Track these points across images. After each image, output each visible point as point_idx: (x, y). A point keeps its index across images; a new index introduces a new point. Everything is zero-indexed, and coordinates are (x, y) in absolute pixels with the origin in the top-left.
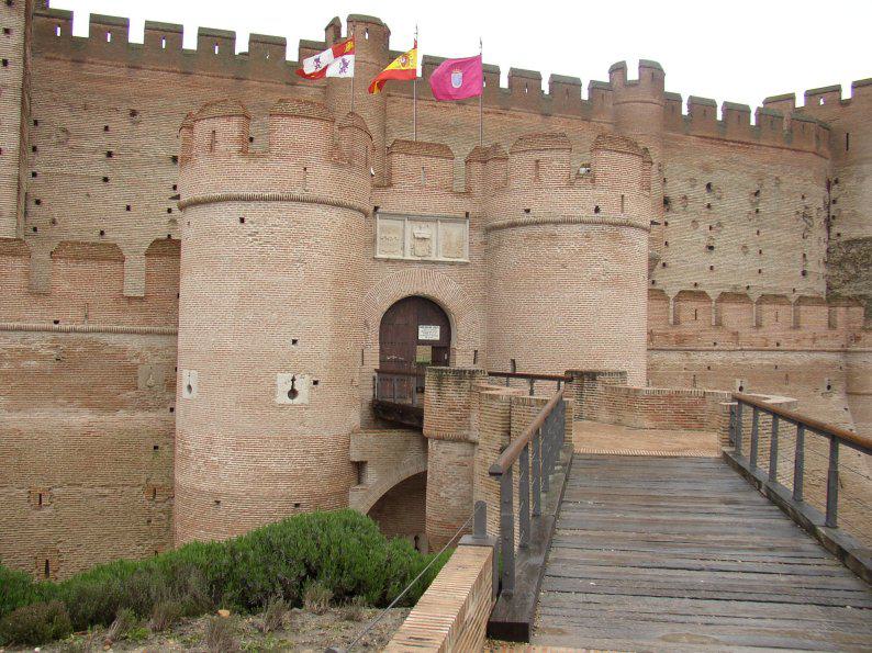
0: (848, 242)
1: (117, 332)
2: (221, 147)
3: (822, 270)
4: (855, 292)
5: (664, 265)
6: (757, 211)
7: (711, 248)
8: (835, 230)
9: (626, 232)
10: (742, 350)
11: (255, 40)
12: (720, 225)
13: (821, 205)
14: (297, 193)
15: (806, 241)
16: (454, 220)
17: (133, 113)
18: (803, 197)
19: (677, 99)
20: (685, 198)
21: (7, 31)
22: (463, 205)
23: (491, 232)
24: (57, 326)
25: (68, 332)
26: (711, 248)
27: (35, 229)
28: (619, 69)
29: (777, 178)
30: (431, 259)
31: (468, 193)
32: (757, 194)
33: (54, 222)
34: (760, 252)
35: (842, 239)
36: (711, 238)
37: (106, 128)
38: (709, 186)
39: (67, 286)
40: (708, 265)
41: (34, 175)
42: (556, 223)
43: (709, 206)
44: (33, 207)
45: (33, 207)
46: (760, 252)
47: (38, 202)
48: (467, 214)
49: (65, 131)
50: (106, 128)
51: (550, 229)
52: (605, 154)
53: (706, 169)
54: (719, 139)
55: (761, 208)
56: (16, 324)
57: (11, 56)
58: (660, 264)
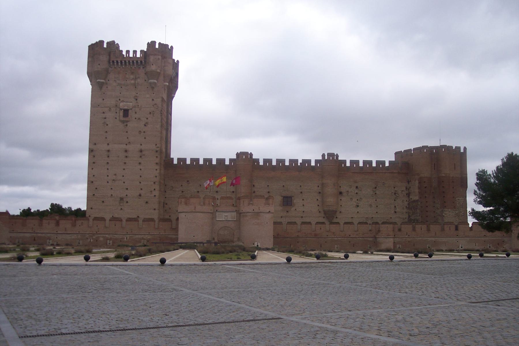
0: (413, 201)
1: (170, 235)
2: (182, 203)
3: (405, 210)
4: (414, 218)
5: (340, 212)
6: (376, 193)
7: (358, 206)
8: (411, 197)
9: (261, 214)
10: (336, 237)
11: (218, 160)
12: (361, 198)
13: (404, 189)
14: (194, 211)
15: (396, 202)
16: (233, 212)
17: (188, 181)
18: (394, 188)
19: (344, 162)
20: (348, 191)
21: (156, 170)
22: (234, 209)
23: (240, 214)
24: (160, 234)
25: (162, 235)
26: (358, 206)
27: (166, 210)
28: (323, 155)
29: (384, 182)
30: (228, 220)
31: (236, 206)
32: (376, 188)
33: (170, 208)
34: (377, 206)
35: (412, 200)
36: (358, 203)
37: (182, 185)
38: (357, 187)
39: (161, 226)
40: (357, 211)
41: (165, 197)
42: (247, 213)
43: (357, 193)
44: (165, 205)
45: (165, 205)
46: (377, 206)
47: (166, 204)
48: (236, 210)
49: (172, 187)
50: (182, 185)
51: (246, 214)
52: (255, 199)
53: (355, 182)
54: (360, 172)
55: (377, 192)
56: (153, 234)
57: (157, 175)
58: (338, 212)
